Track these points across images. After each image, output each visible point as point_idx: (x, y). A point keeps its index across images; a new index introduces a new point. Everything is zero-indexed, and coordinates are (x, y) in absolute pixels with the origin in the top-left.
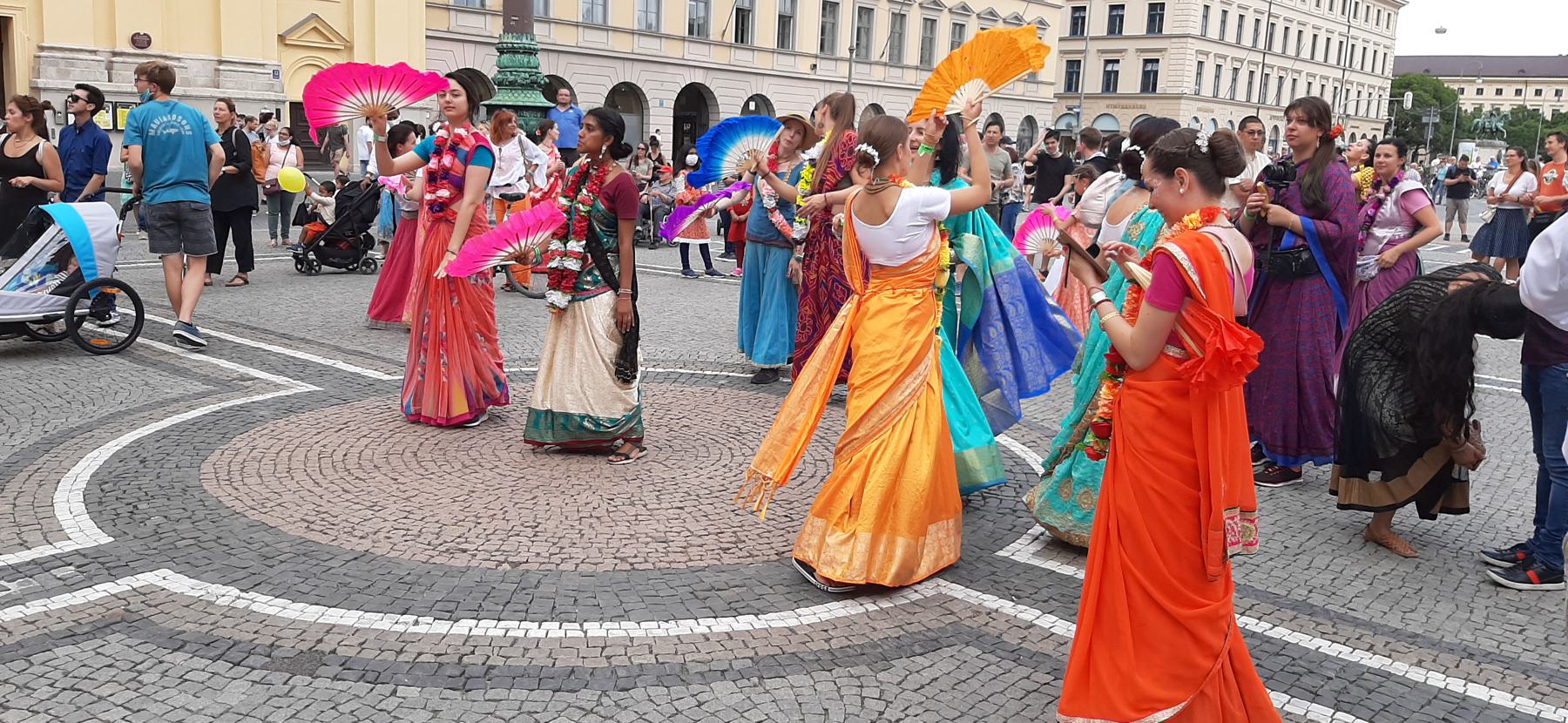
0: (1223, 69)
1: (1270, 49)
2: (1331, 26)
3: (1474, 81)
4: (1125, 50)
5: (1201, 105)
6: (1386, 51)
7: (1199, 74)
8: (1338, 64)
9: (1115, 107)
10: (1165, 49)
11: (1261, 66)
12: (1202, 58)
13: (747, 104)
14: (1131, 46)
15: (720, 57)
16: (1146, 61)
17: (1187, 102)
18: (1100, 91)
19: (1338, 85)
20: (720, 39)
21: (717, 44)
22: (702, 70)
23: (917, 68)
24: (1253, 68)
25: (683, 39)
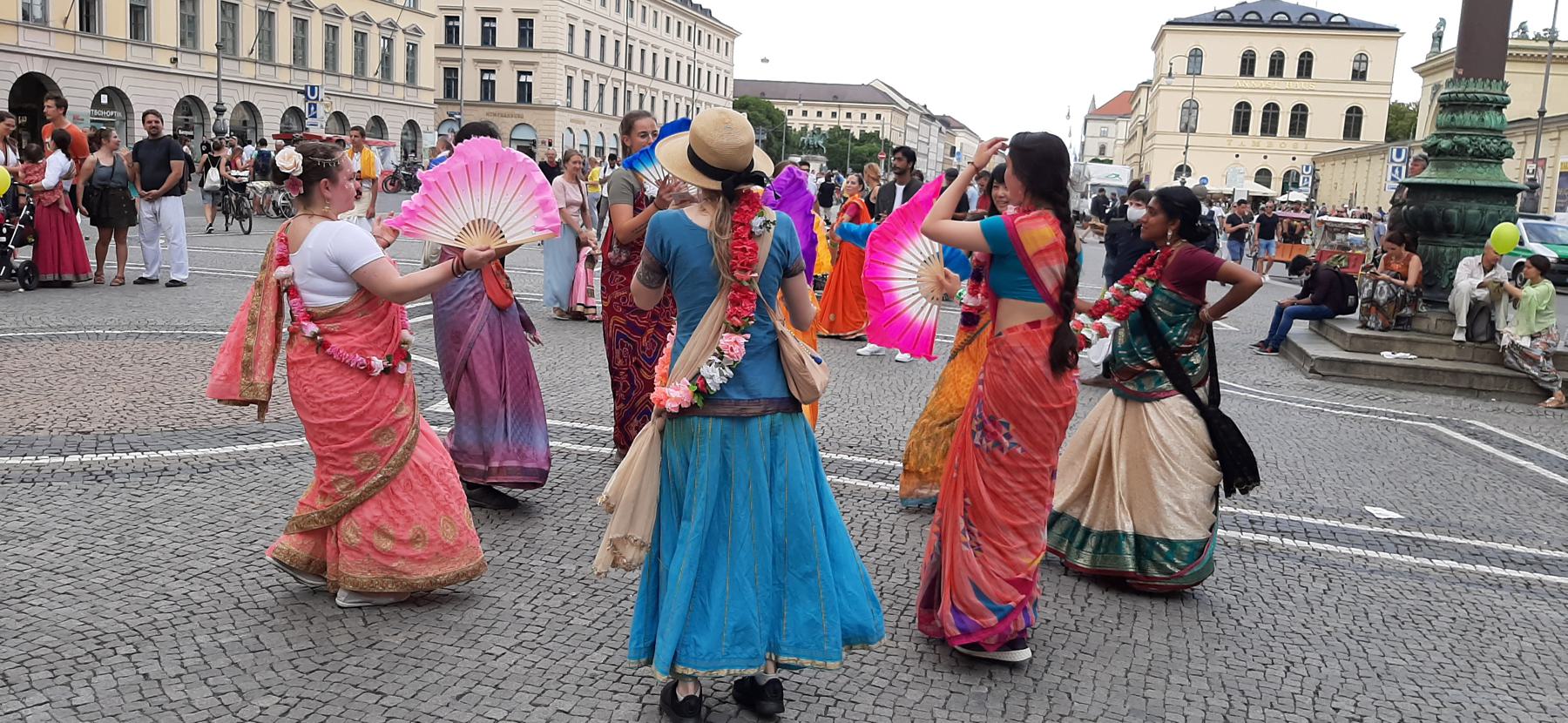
0: (591, 84)
2: (681, 51)
4: (500, 62)
5: (574, 116)
6: (727, 75)
7: (569, 88)
8: (689, 85)
9: (495, 115)
12: (571, 73)
13: (98, 97)
14: (506, 57)
15: (63, 45)
17: (561, 113)
18: (479, 99)
19: (689, 103)
20: (62, 27)
21: (58, 31)
22: (42, 59)
23: (290, 67)
24: (616, 85)
25: (17, 25)
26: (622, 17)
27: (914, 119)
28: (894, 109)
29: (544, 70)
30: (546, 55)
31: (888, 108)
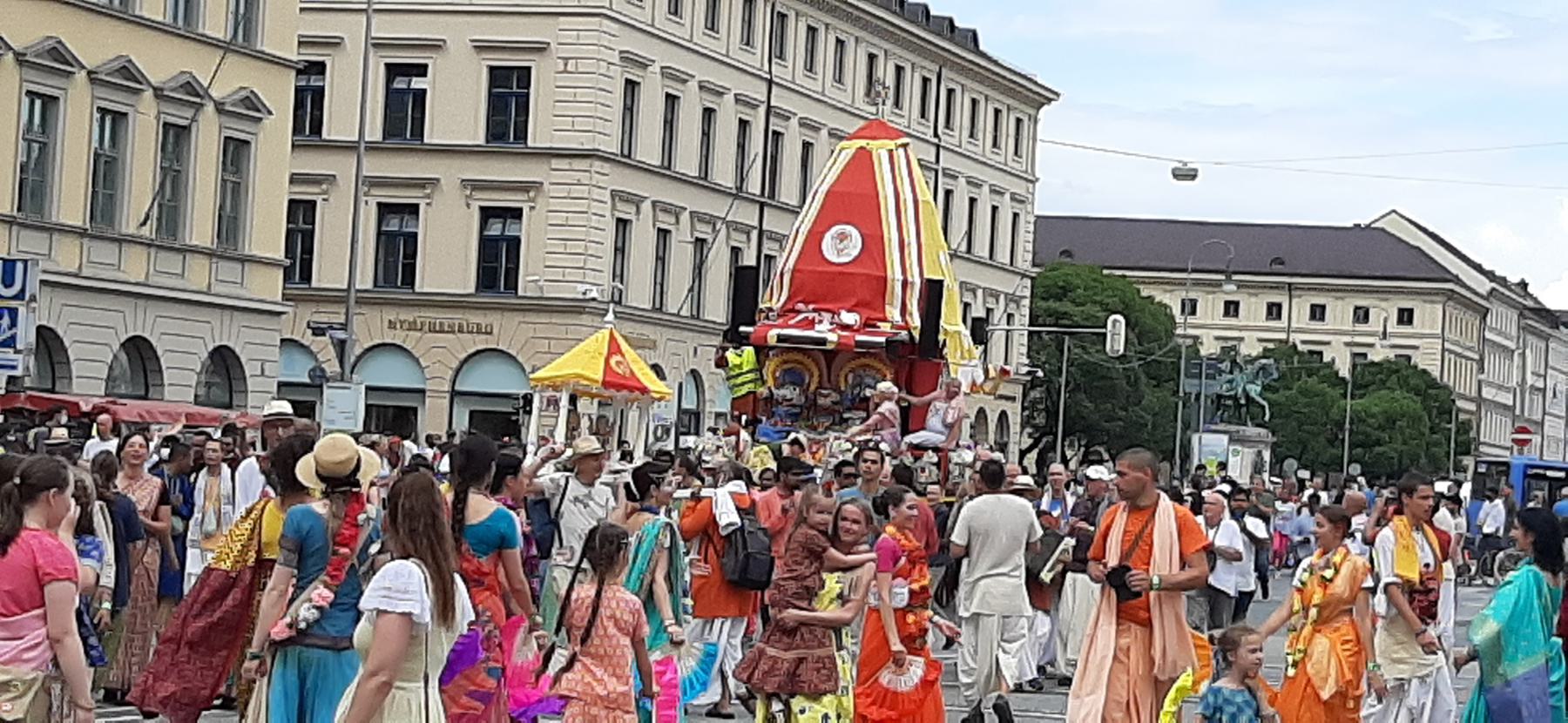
1: (772, 196)
3: (1218, 284)
4: (434, 182)
6: (1018, 208)
7: (620, 250)
9: (412, 327)
10: (537, 186)
11: (754, 235)
14: (449, 172)
16: (487, 214)
26: (756, 58)
27: (1503, 321)
28: (1451, 295)
29: (555, 204)
30: (563, 164)
31: (1437, 292)
